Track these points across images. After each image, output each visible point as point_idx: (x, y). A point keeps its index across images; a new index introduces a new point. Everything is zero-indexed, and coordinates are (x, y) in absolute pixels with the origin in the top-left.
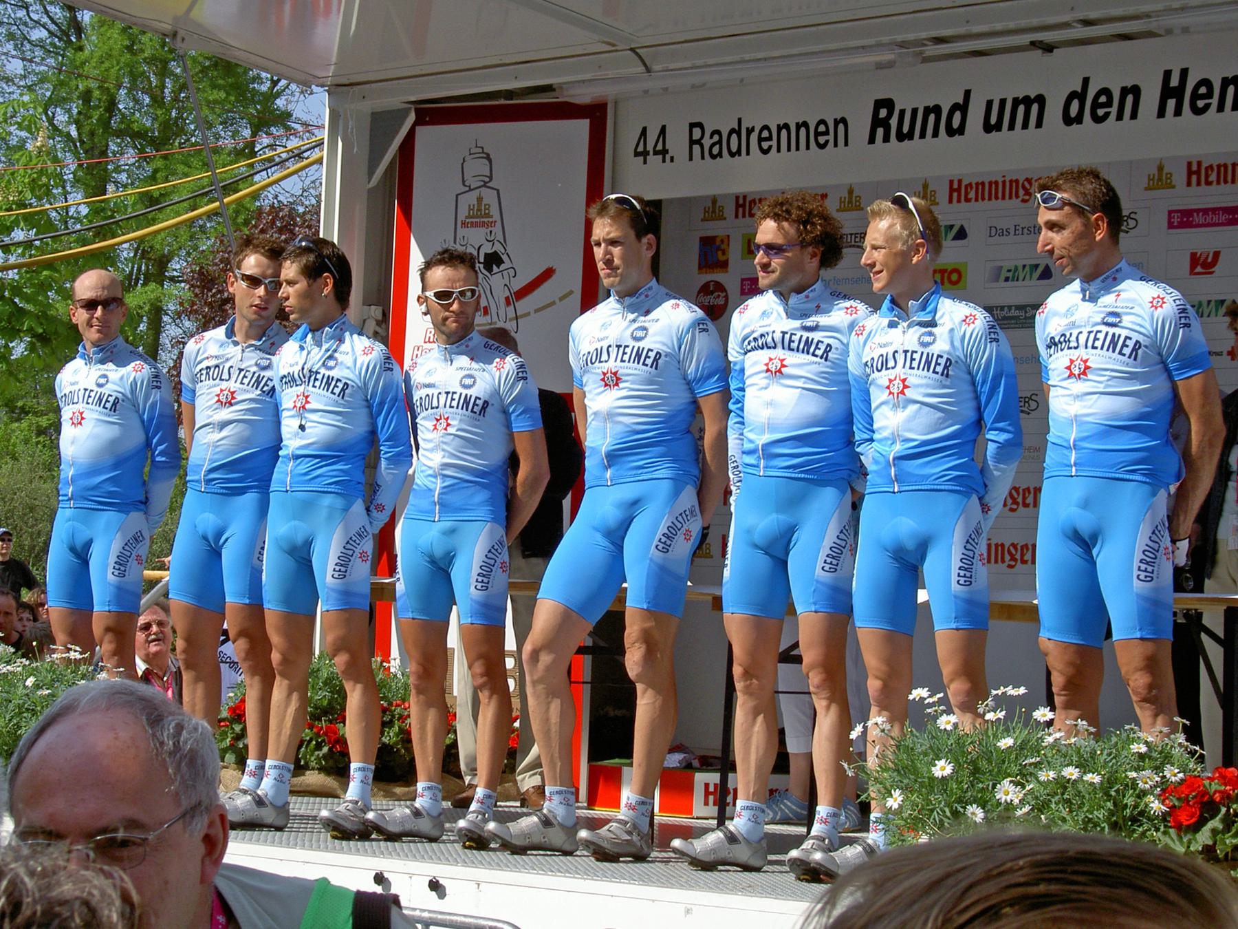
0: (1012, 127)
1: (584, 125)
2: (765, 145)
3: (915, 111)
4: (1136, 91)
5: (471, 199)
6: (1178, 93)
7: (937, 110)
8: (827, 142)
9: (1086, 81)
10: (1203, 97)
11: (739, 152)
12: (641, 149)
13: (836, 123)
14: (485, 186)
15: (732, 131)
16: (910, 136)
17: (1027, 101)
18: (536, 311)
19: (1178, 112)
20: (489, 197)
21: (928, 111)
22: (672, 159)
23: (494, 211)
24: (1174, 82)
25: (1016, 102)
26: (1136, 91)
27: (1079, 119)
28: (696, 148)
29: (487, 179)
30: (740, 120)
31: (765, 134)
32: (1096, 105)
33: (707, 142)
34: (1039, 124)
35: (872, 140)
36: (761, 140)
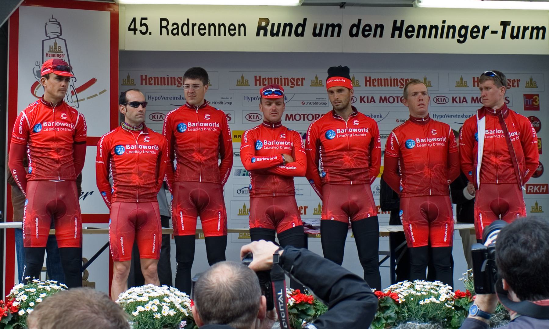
0: (326, 35)
1: (106, 16)
2: (202, 32)
3: (279, 25)
4: (382, 27)
5: (51, 43)
6: (400, 29)
7: (290, 25)
8: (235, 33)
9: (360, 21)
10: (410, 32)
11: (188, 33)
12: (132, 27)
13: (240, 26)
14: (58, 37)
15: (184, 24)
16: (277, 34)
17: (333, 26)
18: (88, 98)
19: (400, 36)
20: (60, 43)
21: (285, 25)
22: (150, 34)
23: (63, 49)
24: (398, 25)
25: (328, 26)
26: (382, 27)
27: (357, 35)
28: (164, 30)
29: (59, 35)
30: (188, 20)
31: (202, 27)
32: (364, 30)
33: (170, 28)
34: (339, 35)
35: (258, 34)
36: (199, 29)
